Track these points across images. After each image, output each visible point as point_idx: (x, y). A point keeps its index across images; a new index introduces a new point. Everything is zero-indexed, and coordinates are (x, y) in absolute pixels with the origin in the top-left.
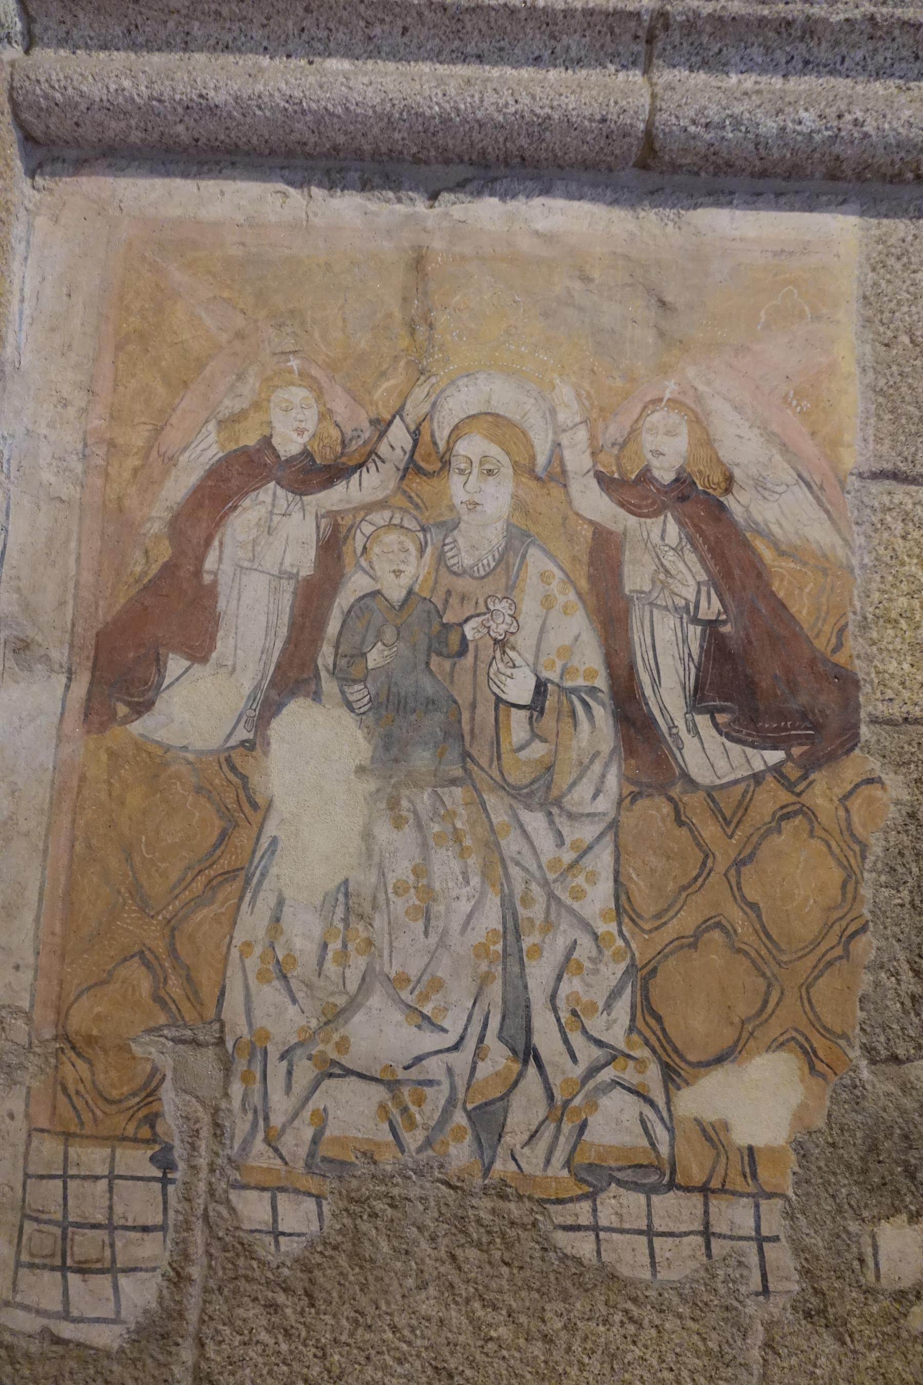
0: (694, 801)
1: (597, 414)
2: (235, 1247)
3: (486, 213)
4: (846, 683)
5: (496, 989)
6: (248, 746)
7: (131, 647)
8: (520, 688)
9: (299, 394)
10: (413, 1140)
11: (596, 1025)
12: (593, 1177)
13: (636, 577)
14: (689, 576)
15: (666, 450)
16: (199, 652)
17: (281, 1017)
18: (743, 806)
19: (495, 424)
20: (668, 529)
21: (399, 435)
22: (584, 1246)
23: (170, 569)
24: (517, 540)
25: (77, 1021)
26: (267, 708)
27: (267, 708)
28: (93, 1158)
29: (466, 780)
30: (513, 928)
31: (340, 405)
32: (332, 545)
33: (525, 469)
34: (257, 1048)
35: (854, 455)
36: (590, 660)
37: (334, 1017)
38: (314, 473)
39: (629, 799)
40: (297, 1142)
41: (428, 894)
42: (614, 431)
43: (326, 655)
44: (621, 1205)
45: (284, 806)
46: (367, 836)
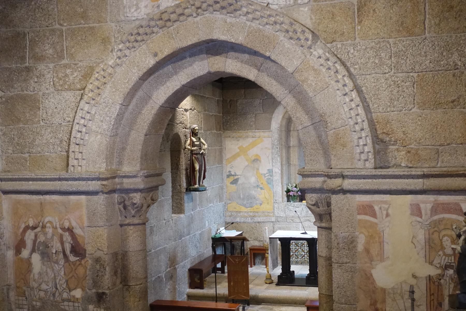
0: (71, 263)
1: (60, 220)
2: (33, 306)
3: (47, 197)
4: (85, 250)
5: (54, 282)
6: (30, 258)
7: (19, 247)
8: (54, 252)
9: (31, 219)
10: (47, 297)
11: (63, 286)
12: (63, 300)
13: (64, 239)
14: (69, 239)
15: (67, 225)
16: (25, 248)
17: (36, 285)
18: (75, 264)
19: (50, 222)
20: (67, 234)
21: (41, 224)
22: (63, 307)
23: (21, 239)
24: (53, 235)
25: (18, 285)
26: (31, 254)
27: (31, 254)
28: (20, 298)
29: (50, 261)
30: (55, 276)
31: (36, 221)
32: (36, 236)
33: (53, 227)
34: (33, 288)
35: (86, 224)
36: (60, 249)
37: (40, 285)
38: (34, 228)
39: (65, 263)
40: (38, 297)
41: (47, 273)
42: (61, 223)
43: (36, 248)
44: (66, 303)
45: (34, 264)
46: (41, 267)
